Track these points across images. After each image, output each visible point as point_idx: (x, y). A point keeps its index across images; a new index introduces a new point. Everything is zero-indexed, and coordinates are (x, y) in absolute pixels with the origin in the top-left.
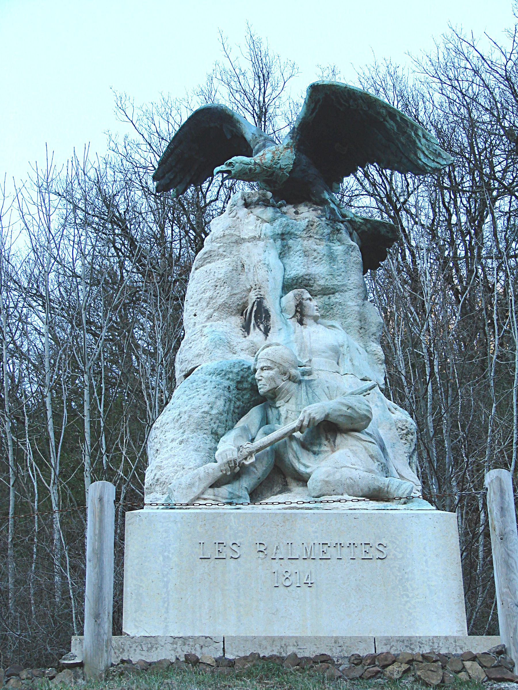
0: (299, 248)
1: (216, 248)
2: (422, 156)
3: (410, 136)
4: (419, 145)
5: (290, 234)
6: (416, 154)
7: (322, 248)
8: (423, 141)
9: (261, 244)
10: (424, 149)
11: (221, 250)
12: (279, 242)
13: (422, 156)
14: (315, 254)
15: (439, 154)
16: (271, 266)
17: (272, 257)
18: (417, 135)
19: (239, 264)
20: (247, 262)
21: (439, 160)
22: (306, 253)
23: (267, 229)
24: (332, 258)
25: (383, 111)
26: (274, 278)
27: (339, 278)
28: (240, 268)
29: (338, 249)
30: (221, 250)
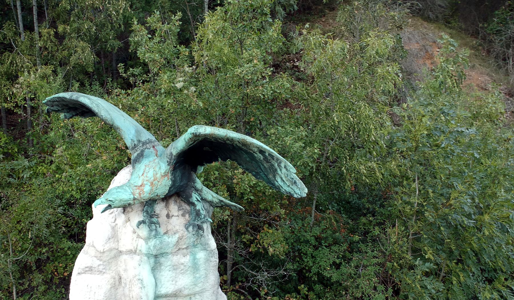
0: (169, 263)
1: (96, 266)
2: (279, 180)
3: (273, 165)
4: (279, 172)
5: (162, 254)
6: (274, 176)
7: (187, 260)
8: (284, 170)
9: (137, 258)
10: (283, 176)
11: (101, 267)
12: (152, 260)
13: (279, 180)
14: (182, 267)
15: (295, 182)
16: (145, 283)
17: (145, 271)
18: (279, 166)
19: (117, 278)
20: (124, 276)
21: (294, 187)
22: (175, 267)
23: (143, 246)
24: (195, 267)
25: (256, 150)
26: (147, 295)
27: (200, 285)
28: (117, 283)
29: (201, 255)
30: (101, 267)
